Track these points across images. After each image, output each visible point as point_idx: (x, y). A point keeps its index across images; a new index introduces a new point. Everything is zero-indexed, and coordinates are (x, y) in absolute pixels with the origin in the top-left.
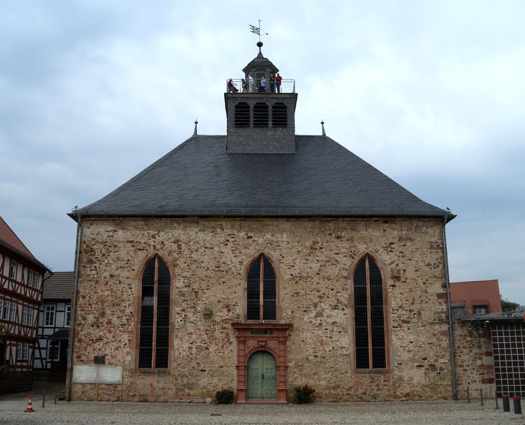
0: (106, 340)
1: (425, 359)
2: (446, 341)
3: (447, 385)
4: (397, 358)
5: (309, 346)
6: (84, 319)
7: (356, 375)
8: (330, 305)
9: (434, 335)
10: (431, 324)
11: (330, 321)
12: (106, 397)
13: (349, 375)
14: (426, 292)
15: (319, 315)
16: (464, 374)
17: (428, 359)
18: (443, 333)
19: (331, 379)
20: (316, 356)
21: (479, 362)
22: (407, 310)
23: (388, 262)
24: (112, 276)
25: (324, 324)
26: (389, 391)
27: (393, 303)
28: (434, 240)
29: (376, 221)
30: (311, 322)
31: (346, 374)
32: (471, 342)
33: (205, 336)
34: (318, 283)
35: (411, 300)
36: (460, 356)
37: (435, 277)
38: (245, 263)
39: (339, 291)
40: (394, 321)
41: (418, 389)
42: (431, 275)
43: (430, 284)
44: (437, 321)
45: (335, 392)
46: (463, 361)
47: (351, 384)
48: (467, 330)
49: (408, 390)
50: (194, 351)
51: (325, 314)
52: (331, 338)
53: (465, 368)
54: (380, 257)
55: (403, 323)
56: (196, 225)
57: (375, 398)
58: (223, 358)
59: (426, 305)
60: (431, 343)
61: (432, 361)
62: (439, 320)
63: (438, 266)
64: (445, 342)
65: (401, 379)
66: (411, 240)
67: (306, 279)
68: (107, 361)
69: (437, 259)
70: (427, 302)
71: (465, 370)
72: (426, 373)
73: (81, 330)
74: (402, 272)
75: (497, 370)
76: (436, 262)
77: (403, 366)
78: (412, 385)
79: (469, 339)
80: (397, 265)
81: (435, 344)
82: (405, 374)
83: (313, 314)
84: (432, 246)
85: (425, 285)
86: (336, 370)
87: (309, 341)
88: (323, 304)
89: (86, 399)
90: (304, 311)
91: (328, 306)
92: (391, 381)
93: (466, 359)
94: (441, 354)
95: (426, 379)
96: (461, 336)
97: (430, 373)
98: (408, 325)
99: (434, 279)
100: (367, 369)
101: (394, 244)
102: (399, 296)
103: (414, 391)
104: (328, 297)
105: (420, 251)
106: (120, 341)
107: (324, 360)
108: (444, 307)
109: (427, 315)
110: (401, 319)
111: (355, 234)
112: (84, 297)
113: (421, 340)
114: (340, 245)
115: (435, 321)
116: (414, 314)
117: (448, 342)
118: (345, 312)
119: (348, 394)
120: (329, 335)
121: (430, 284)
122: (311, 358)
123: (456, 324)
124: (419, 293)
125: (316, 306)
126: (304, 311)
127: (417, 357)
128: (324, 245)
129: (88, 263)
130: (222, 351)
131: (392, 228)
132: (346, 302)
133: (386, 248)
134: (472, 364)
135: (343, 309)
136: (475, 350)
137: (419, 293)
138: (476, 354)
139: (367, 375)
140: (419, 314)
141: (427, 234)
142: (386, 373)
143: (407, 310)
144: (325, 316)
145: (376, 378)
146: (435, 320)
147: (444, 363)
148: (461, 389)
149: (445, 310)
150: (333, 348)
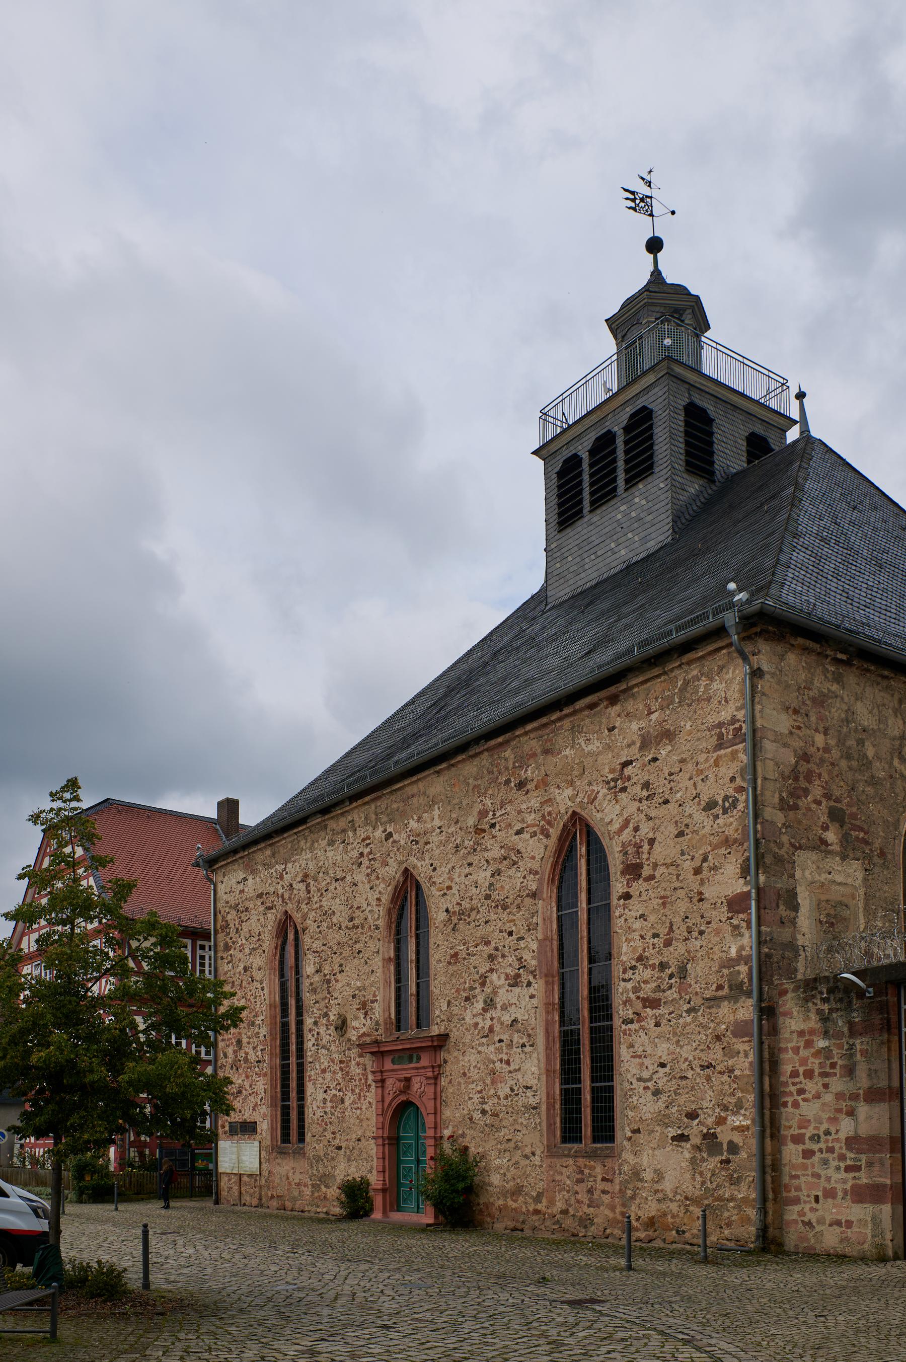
1: (693, 1115)
2: (746, 1056)
3: (745, 1200)
4: (631, 1114)
5: (473, 1086)
7: (549, 1160)
8: (507, 977)
9: (718, 1038)
10: (713, 1001)
11: (507, 1018)
13: (537, 1160)
14: (701, 900)
15: (489, 1004)
16: (805, 1167)
17: (702, 1116)
18: (740, 1030)
19: (508, 1170)
20: (484, 1112)
21: (846, 1127)
22: (653, 967)
23: (616, 826)
25: (497, 1028)
26: (613, 1208)
27: (624, 949)
29: (592, 706)
31: (532, 1158)
32: (826, 1053)
34: (486, 922)
35: (663, 931)
36: (796, 1105)
37: (727, 842)
38: (383, 900)
39: (522, 934)
40: (625, 1003)
41: (674, 1207)
42: (715, 840)
43: (710, 869)
44: (726, 991)
45: (514, 1205)
46: (804, 1123)
47: (541, 1186)
48: (819, 1012)
49: (651, 1208)
51: (499, 1002)
52: (508, 1063)
53: (809, 1145)
54: (599, 815)
55: (645, 1007)
56: (323, 834)
57: (585, 1227)
58: (361, 1121)
59: (698, 943)
60: (709, 1066)
61: (710, 1121)
62: (730, 987)
64: (744, 1062)
65: (636, 1174)
66: (668, 735)
67: (469, 916)
69: (733, 779)
70: (701, 933)
71: (808, 1154)
72: (693, 1161)
74: (646, 847)
76: (731, 792)
77: (642, 1138)
78: (660, 1195)
79: (822, 1043)
80: (636, 829)
81: (718, 1068)
82: (645, 1160)
83: (480, 1005)
84: (720, 736)
85: (698, 877)
86: (517, 1148)
87: (474, 1074)
88: (494, 976)
91: (502, 981)
92: (617, 1181)
93: (810, 1116)
94: (733, 1100)
95: (694, 1179)
96: (801, 1033)
97: (703, 1160)
98: (657, 1012)
99: (723, 851)
100: (576, 1146)
101: (631, 762)
102: (637, 925)
103: (665, 1215)
104: (503, 956)
105: (690, 767)
108: (748, 940)
109: (704, 976)
110: (641, 994)
111: (552, 763)
113: (685, 1055)
114: (524, 806)
115: (720, 993)
116: (671, 976)
117: (751, 1058)
118: (532, 990)
119: (537, 1212)
120: (505, 1057)
121: (711, 869)
122: (477, 1116)
123: (790, 995)
124: (683, 906)
127: (674, 1110)
128: (498, 814)
130: (359, 1105)
131: (627, 715)
132: (534, 963)
133: (612, 784)
134: (827, 1133)
136: (838, 1084)
137: (683, 906)
138: (839, 1096)
139: (571, 1161)
140: (683, 972)
141: (709, 700)
142: (607, 1157)
143: (653, 967)
144: (499, 1006)
145: (587, 1171)
146: (720, 987)
147: (741, 1129)
148: (795, 1217)
150: (512, 1090)
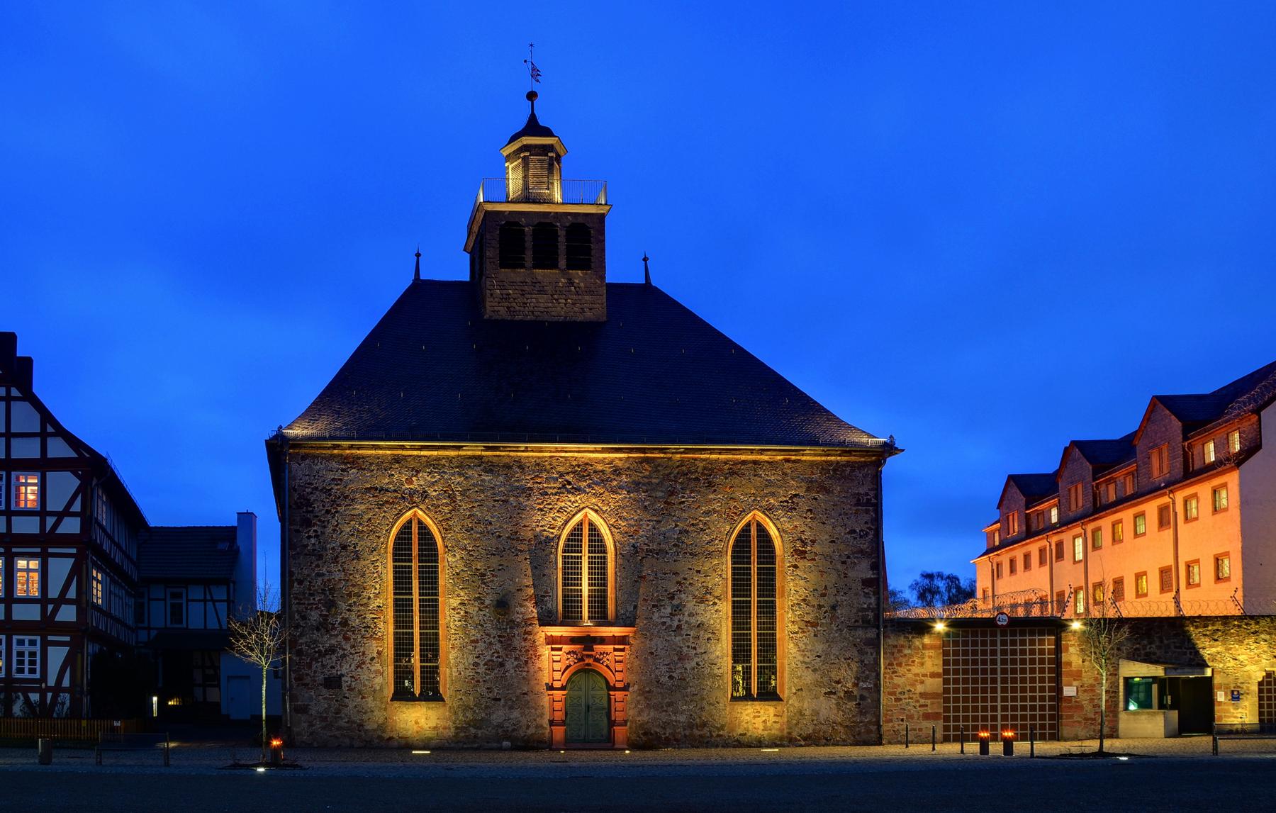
0: (341, 652)
1: (838, 682)
6: (304, 618)
12: (347, 741)
20: (671, 677)
24: (344, 547)
25: (685, 627)
28: (862, 491)
30: (664, 623)
33: (499, 645)
50: (482, 669)
53: (899, 696)
63: (867, 534)
68: (344, 685)
72: (838, 704)
73: (301, 635)
75: (946, 700)
83: (669, 610)
88: (683, 596)
89: (315, 745)
90: (654, 606)
106: (364, 653)
107: (684, 683)
112: (300, 582)
122: (664, 679)
125: (672, 598)
126: (654, 606)
129: (301, 525)
135: (715, 604)
149: (873, 606)
